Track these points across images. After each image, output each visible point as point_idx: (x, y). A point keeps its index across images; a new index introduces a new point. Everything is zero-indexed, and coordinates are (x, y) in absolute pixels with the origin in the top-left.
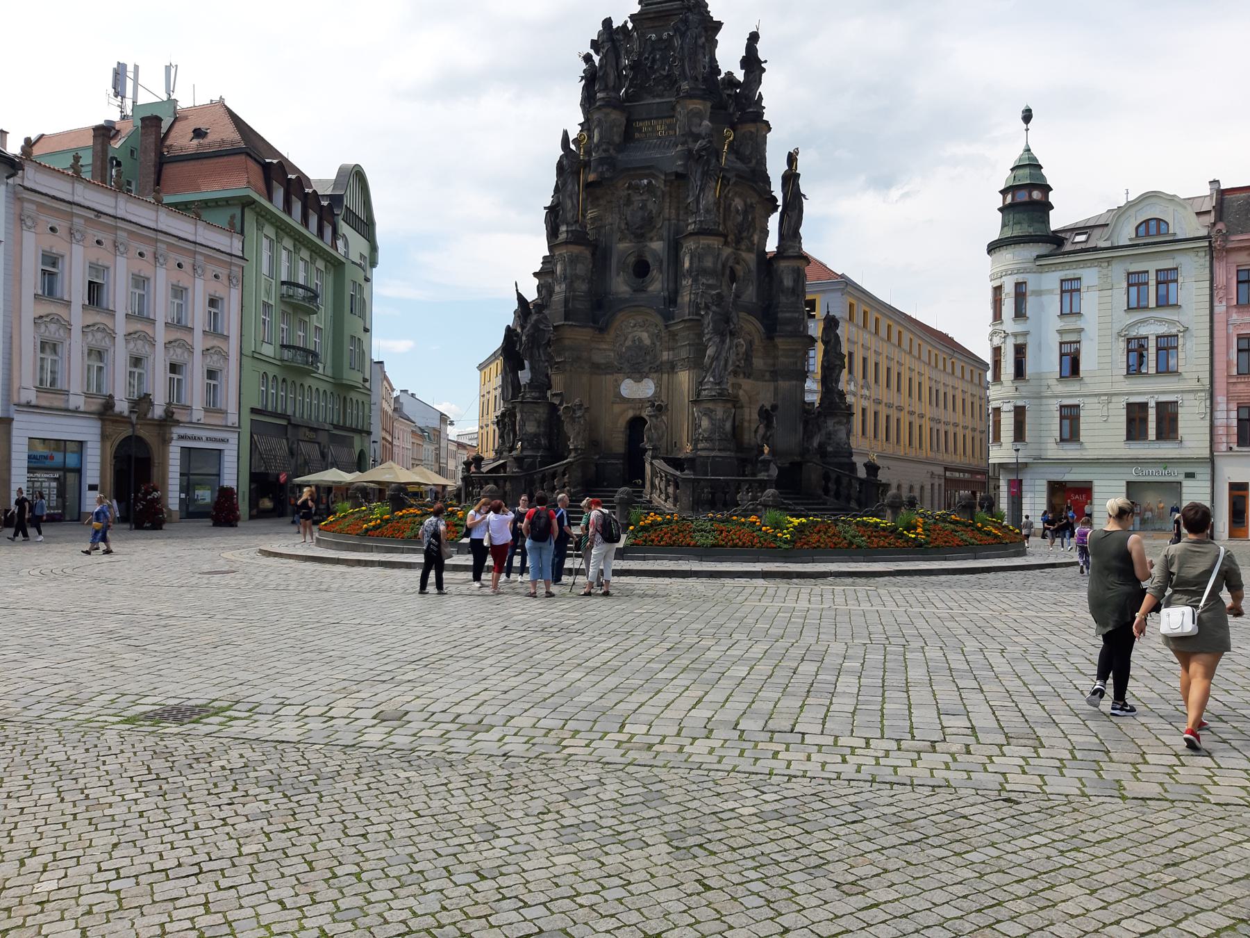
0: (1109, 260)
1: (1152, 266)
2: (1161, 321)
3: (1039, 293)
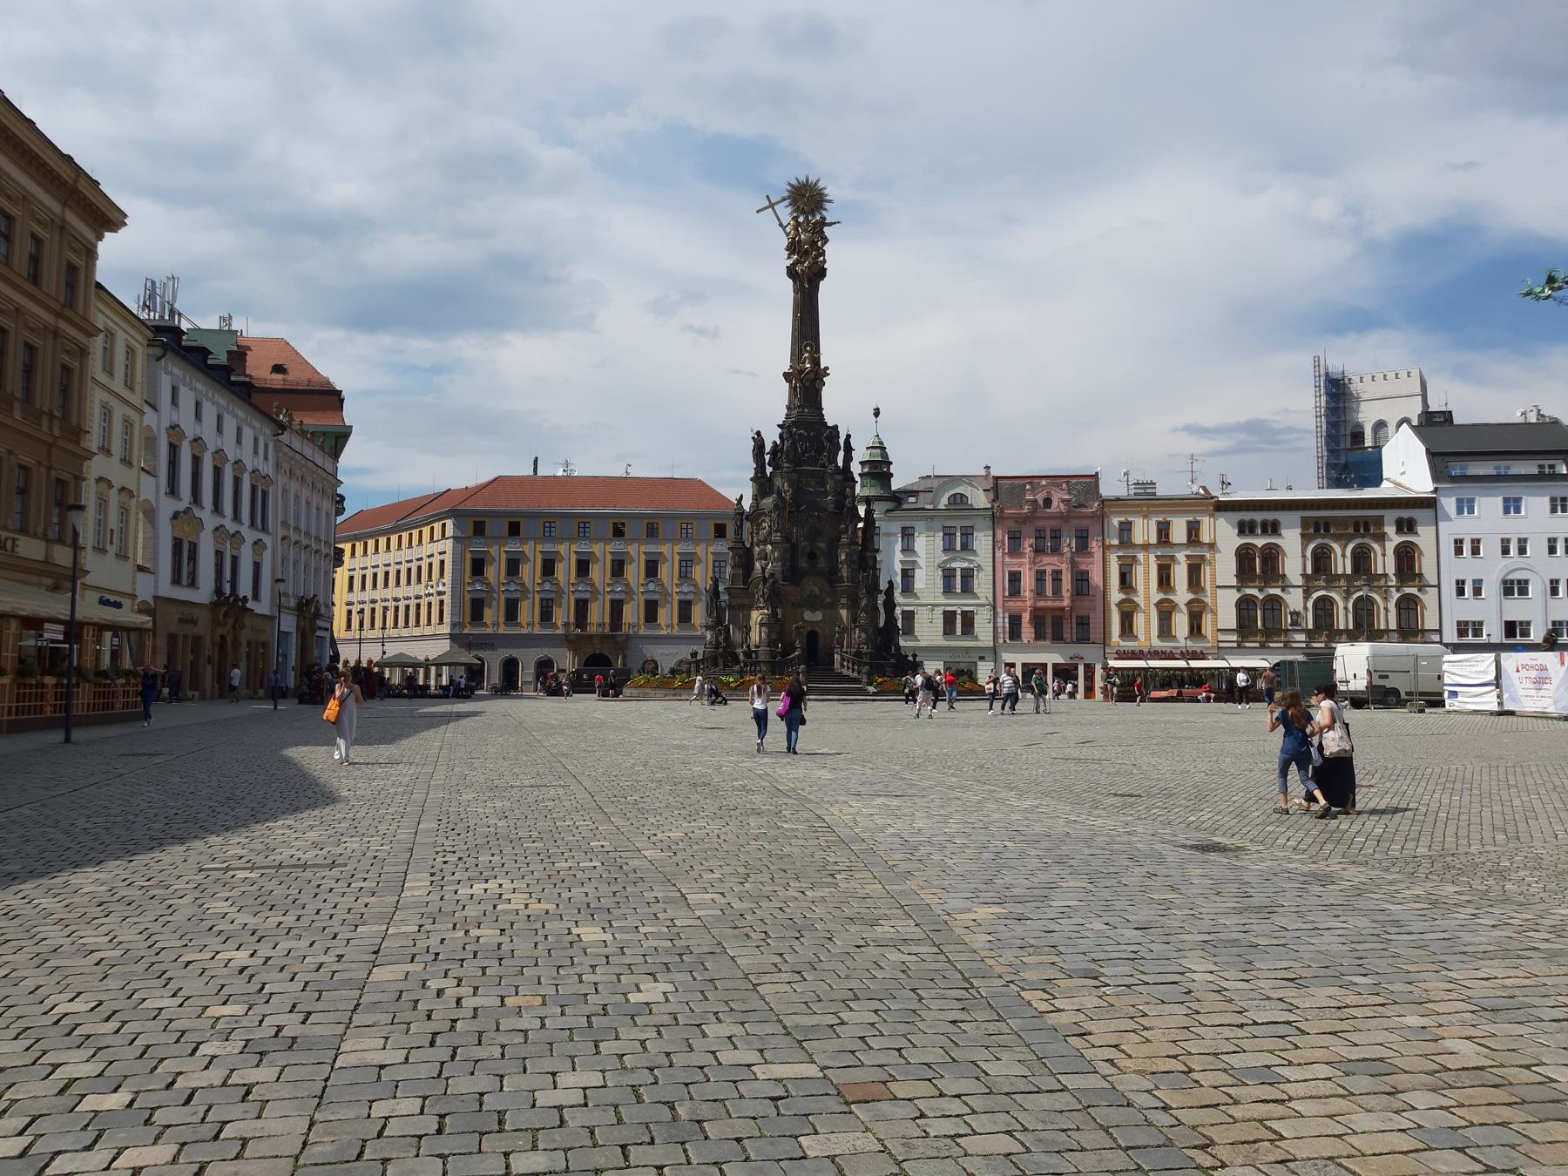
0: (932, 518)
1: (959, 524)
2: (964, 560)
3: (888, 535)
